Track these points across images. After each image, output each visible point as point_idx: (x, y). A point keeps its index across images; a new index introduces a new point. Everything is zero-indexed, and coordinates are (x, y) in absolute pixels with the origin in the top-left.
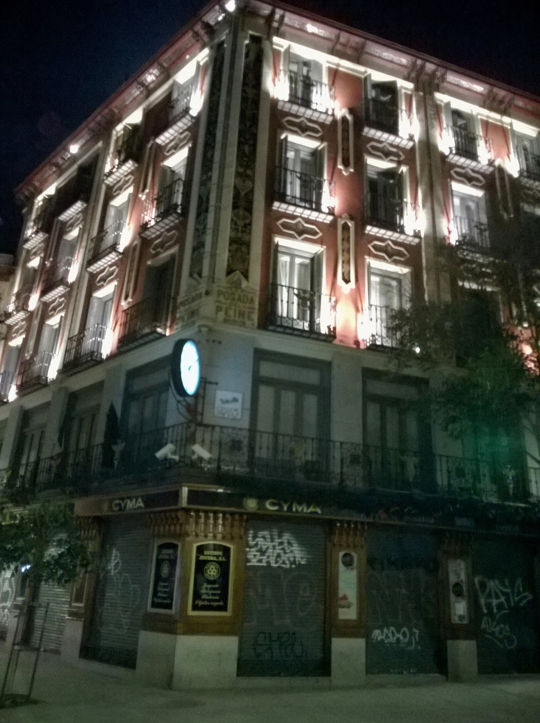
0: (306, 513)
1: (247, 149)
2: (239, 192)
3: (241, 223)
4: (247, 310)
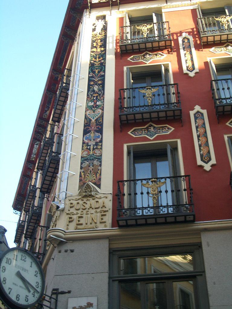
1: (96, 88)
2: (90, 120)
3: (92, 143)
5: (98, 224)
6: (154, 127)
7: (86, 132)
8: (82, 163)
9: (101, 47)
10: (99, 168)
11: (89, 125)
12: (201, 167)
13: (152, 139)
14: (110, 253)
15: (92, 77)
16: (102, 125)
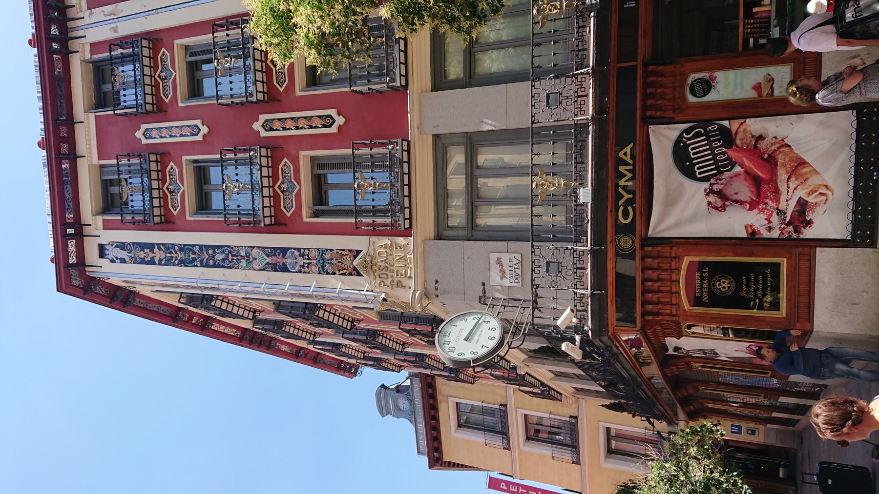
0: (634, 165)
1: (219, 257)
2: (268, 263)
3: (300, 261)
6: (282, 183)
7: (284, 269)
8: (328, 273)
9: (152, 251)
10: (335, 251)
11: (275, 265)
12: (340, 127)
13: (298, 187)
14: (440, 239)
15: (201, 262)
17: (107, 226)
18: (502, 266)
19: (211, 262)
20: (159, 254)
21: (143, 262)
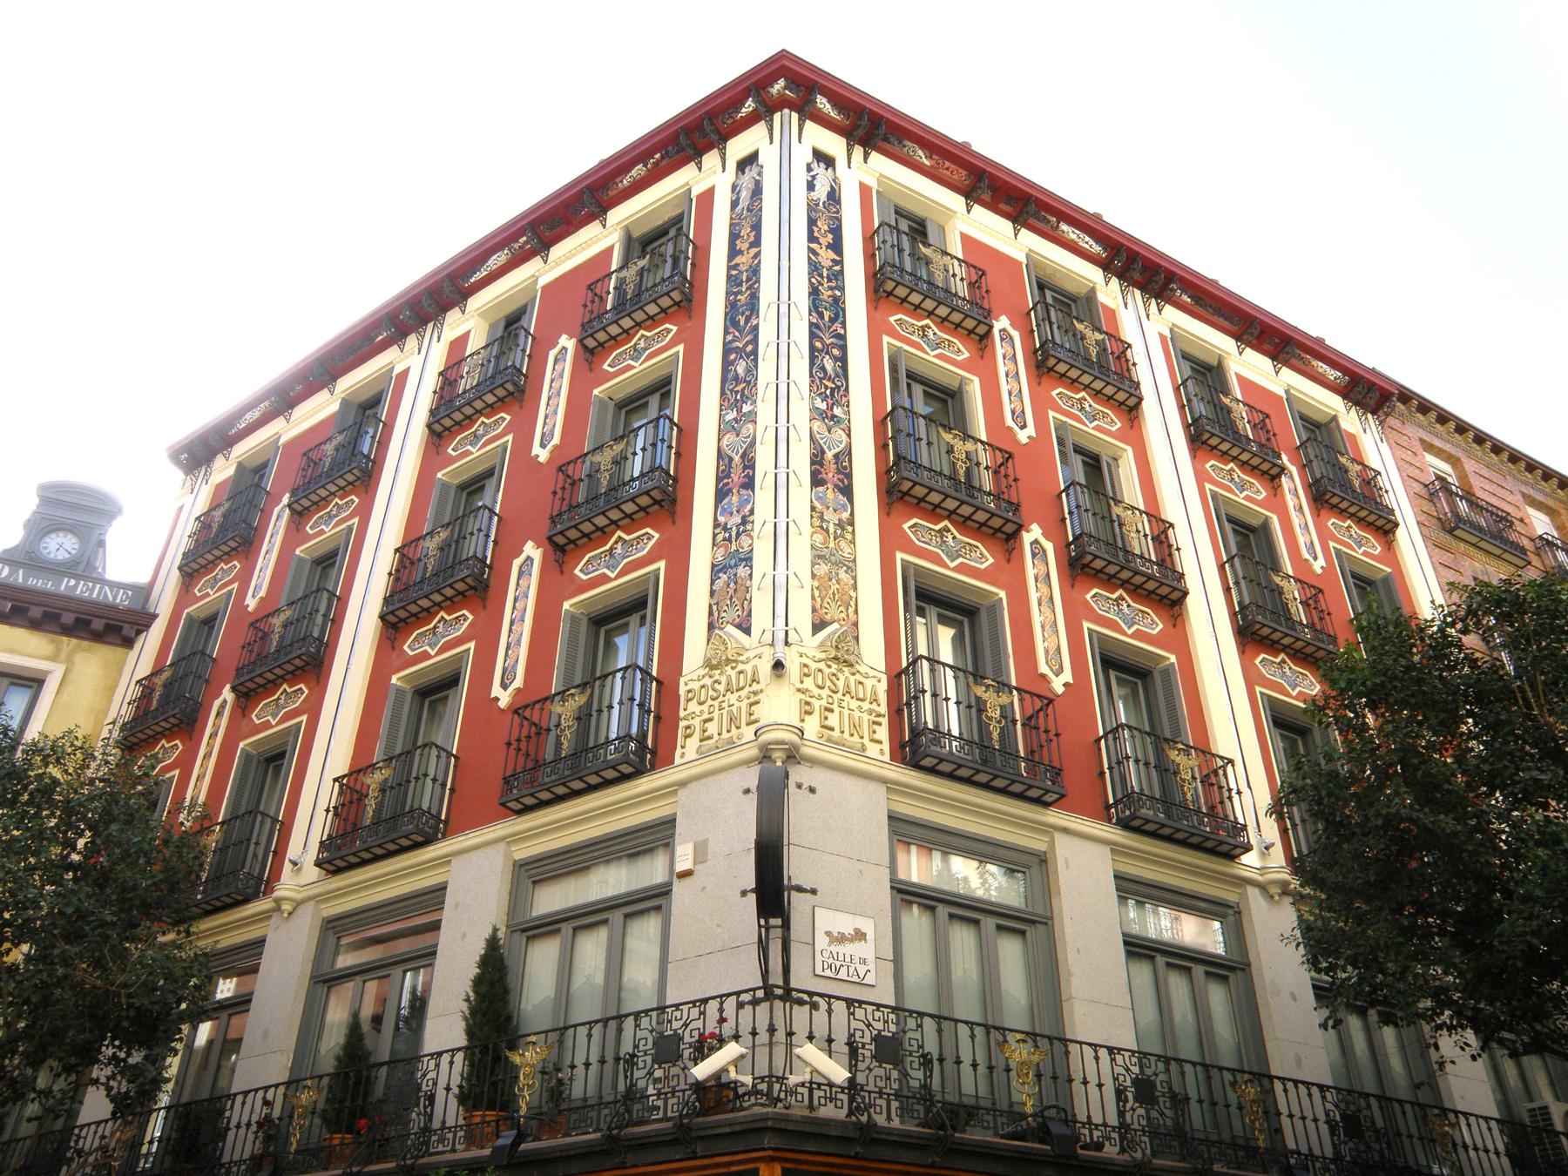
1: (829, 364)
2: (823, 452)
4: (866, 717)
5: (866, 740)
7: (817, 481)
9: (829, 246)
16: (849, 476)
17: (865, 190)
18: (851, 940)
19: (818, 345)
20: (826, 256)
21: (812, 222)
